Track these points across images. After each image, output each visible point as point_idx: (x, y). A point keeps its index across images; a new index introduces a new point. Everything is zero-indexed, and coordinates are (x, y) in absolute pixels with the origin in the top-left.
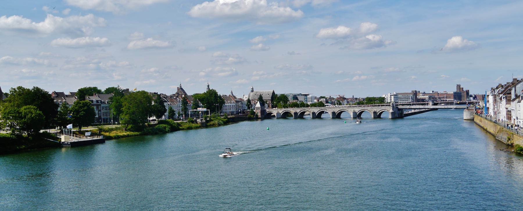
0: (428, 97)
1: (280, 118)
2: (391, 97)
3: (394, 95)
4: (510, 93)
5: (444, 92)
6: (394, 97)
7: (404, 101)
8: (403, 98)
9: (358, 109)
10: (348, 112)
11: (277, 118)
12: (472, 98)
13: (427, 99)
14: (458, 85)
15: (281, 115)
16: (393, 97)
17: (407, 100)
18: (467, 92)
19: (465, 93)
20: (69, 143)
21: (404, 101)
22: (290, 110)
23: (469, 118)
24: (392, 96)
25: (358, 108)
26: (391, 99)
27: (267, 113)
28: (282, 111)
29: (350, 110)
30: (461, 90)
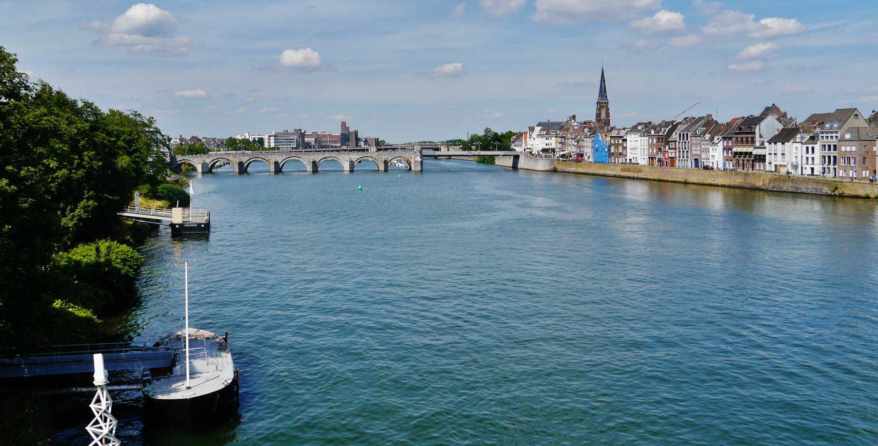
0: (314, 139)
1: (206, 172)
2: (269, 139)
3: (275, 136)
4: (754, 133)
5: (323, 132)
6: (275, 139)
7: (285, 146)
8: (283, 140)
9: (357, 156)
10: (339, 160)
11: (203, 173)
12: (362, 143)
13: (313, 143)
14: (343, 122)
15: (209, 166)
16: (272, 139)
17: (290, 145)
18: (356, 133)
19: (354, 136)
20: (203, 226)
21: (285, 146)
22: (229, 158)
23: (548, 168)
24: (271, 138)
25: (356, 155)
26: (269, 142)
27: (179, 163)
28: (211, 160)
29: (343, 158)
30: (347, 130)
